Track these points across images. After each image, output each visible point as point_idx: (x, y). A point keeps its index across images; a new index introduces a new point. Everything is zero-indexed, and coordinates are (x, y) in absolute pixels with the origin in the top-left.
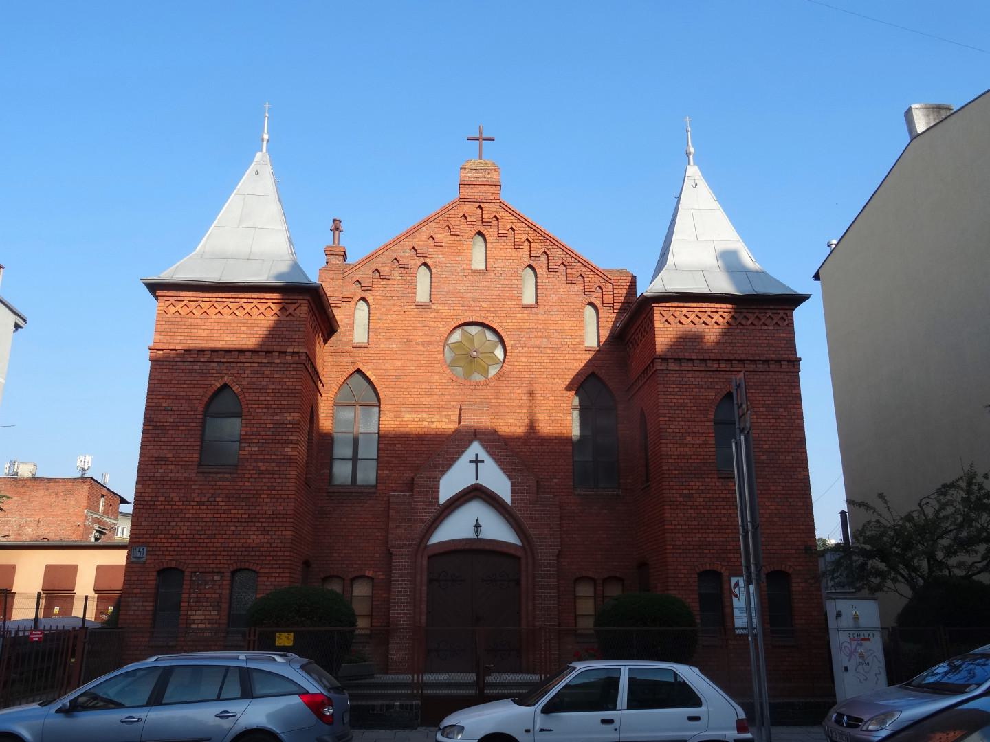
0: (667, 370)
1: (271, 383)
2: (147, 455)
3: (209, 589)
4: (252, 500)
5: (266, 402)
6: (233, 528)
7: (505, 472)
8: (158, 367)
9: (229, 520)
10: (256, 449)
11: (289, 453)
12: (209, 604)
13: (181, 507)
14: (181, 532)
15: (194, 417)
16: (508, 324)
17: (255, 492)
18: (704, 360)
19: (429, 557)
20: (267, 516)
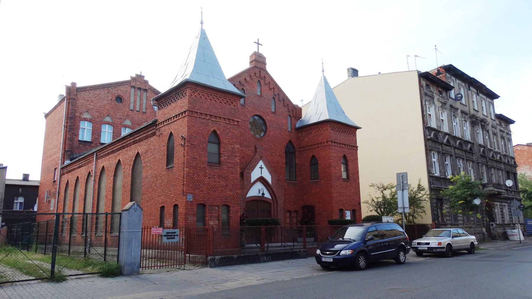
0: (332, 145)
1: (230, 132)
2: (190, 156)
3: (215, 212)
4: (226, 178)
5: (228, 139)
6: (221, 189)
7: (269, 173)
8: (190, 118)
9: (219, 185)
10: (226, 158)
11: (237, 161)
12: (214, 218)
13: (203, 179)
14: (204, 189)
15: (205, 142)
16: (268, 118)
17: (227, 175)
18: (340, 143)
19: (246, 202)
20: (232, 185)
